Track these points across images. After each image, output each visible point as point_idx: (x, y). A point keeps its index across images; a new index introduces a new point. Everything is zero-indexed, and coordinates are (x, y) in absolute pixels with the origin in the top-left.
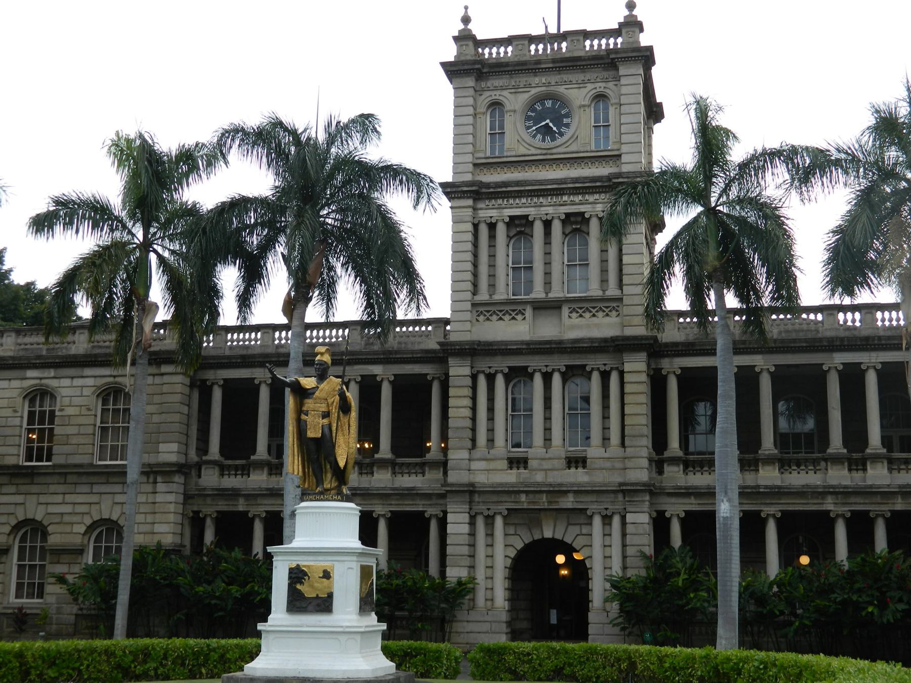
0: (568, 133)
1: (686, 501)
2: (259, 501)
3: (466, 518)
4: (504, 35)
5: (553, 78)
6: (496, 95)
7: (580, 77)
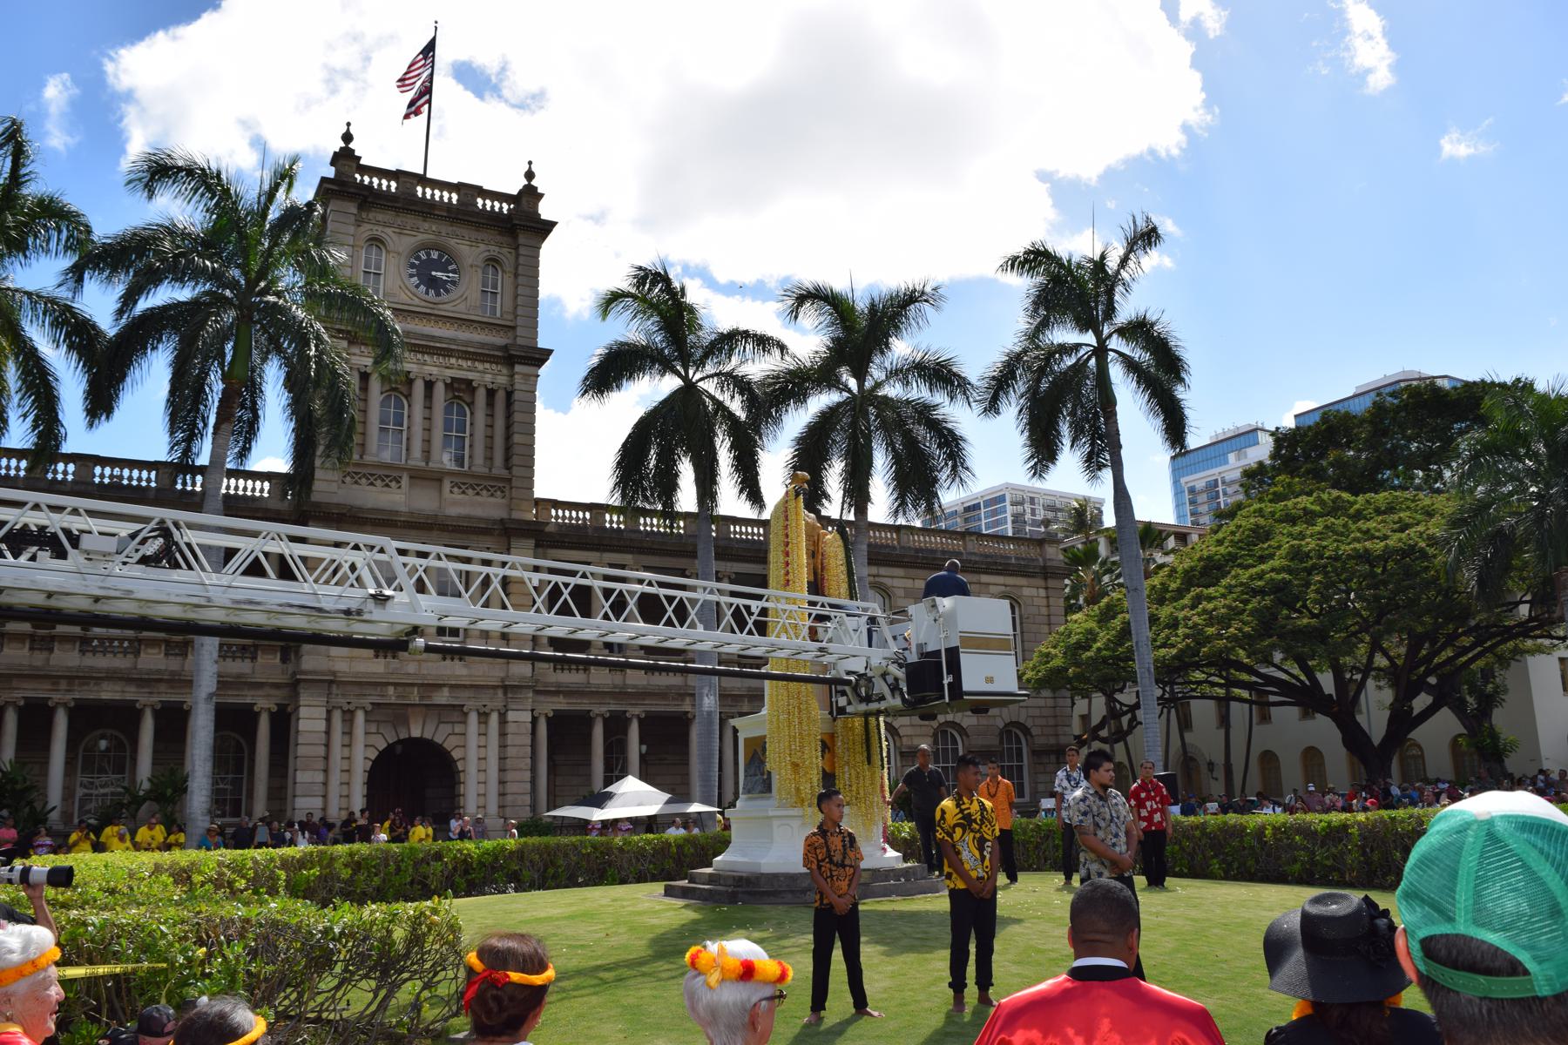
0: (456, 293)
1: (555, 699)
2: (15, 683)
3: (322, 712)
4: (391, 166)
5: (445, 228)
6: (378, 231)
7: (474, 235)
